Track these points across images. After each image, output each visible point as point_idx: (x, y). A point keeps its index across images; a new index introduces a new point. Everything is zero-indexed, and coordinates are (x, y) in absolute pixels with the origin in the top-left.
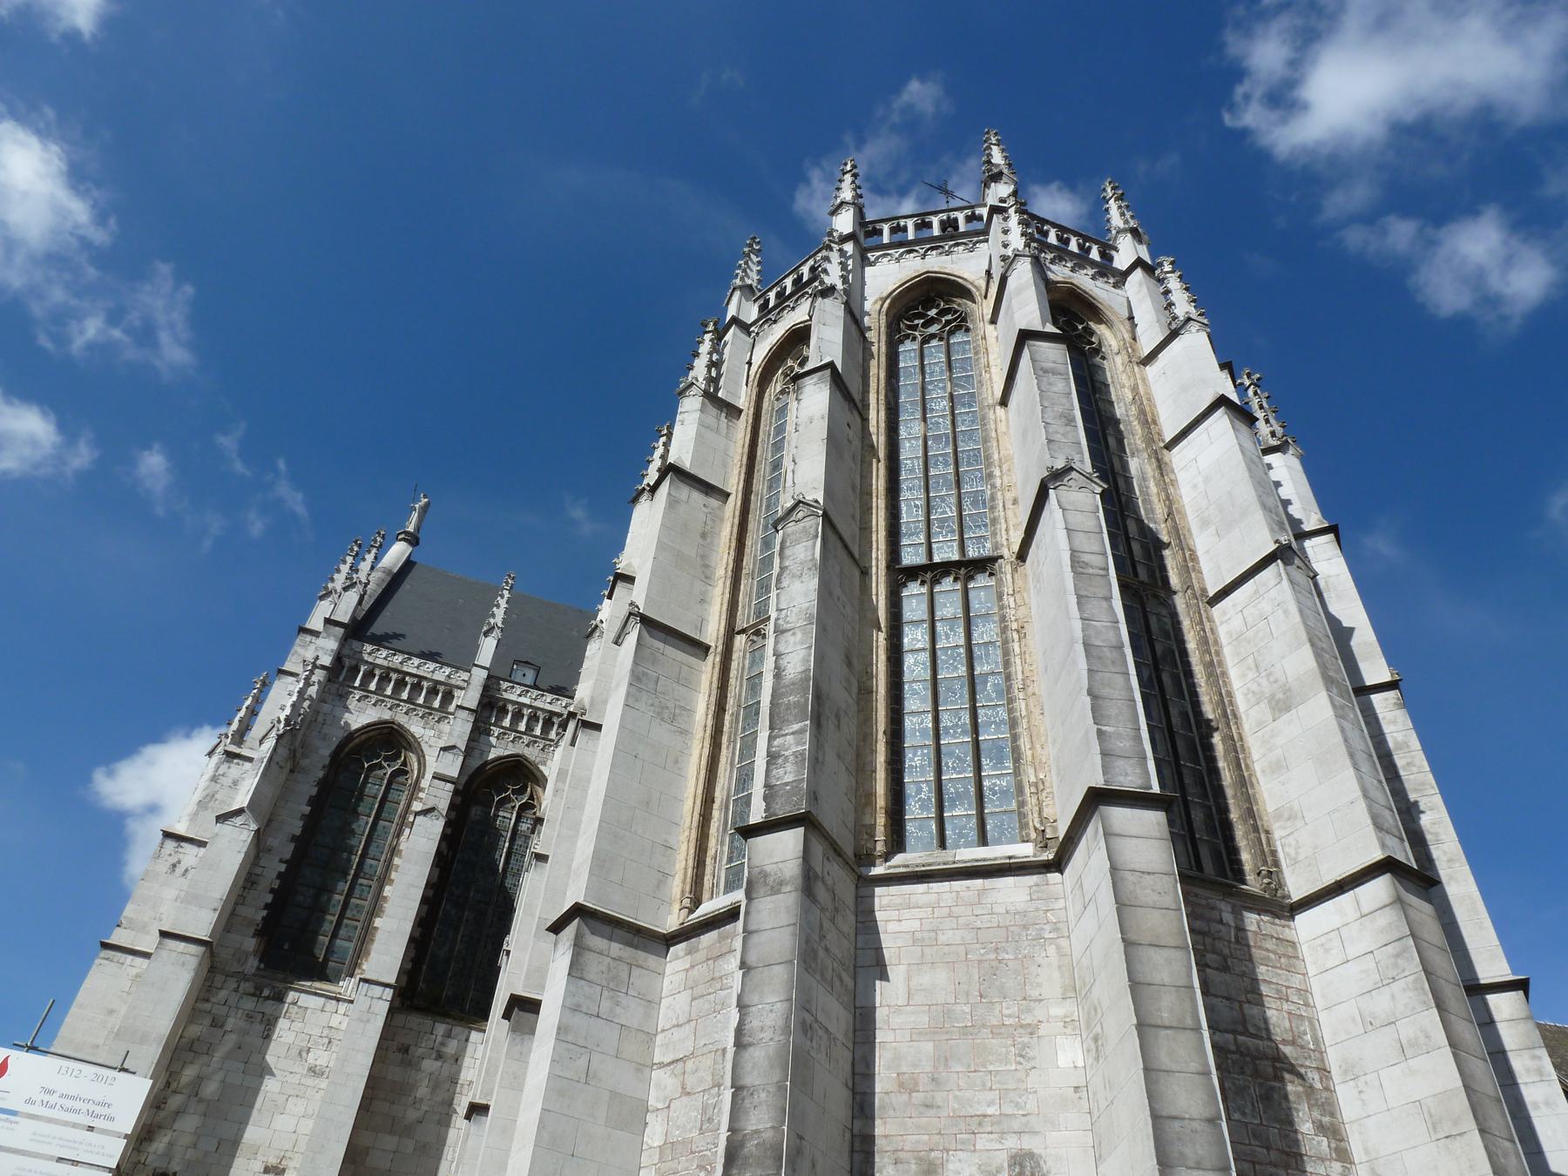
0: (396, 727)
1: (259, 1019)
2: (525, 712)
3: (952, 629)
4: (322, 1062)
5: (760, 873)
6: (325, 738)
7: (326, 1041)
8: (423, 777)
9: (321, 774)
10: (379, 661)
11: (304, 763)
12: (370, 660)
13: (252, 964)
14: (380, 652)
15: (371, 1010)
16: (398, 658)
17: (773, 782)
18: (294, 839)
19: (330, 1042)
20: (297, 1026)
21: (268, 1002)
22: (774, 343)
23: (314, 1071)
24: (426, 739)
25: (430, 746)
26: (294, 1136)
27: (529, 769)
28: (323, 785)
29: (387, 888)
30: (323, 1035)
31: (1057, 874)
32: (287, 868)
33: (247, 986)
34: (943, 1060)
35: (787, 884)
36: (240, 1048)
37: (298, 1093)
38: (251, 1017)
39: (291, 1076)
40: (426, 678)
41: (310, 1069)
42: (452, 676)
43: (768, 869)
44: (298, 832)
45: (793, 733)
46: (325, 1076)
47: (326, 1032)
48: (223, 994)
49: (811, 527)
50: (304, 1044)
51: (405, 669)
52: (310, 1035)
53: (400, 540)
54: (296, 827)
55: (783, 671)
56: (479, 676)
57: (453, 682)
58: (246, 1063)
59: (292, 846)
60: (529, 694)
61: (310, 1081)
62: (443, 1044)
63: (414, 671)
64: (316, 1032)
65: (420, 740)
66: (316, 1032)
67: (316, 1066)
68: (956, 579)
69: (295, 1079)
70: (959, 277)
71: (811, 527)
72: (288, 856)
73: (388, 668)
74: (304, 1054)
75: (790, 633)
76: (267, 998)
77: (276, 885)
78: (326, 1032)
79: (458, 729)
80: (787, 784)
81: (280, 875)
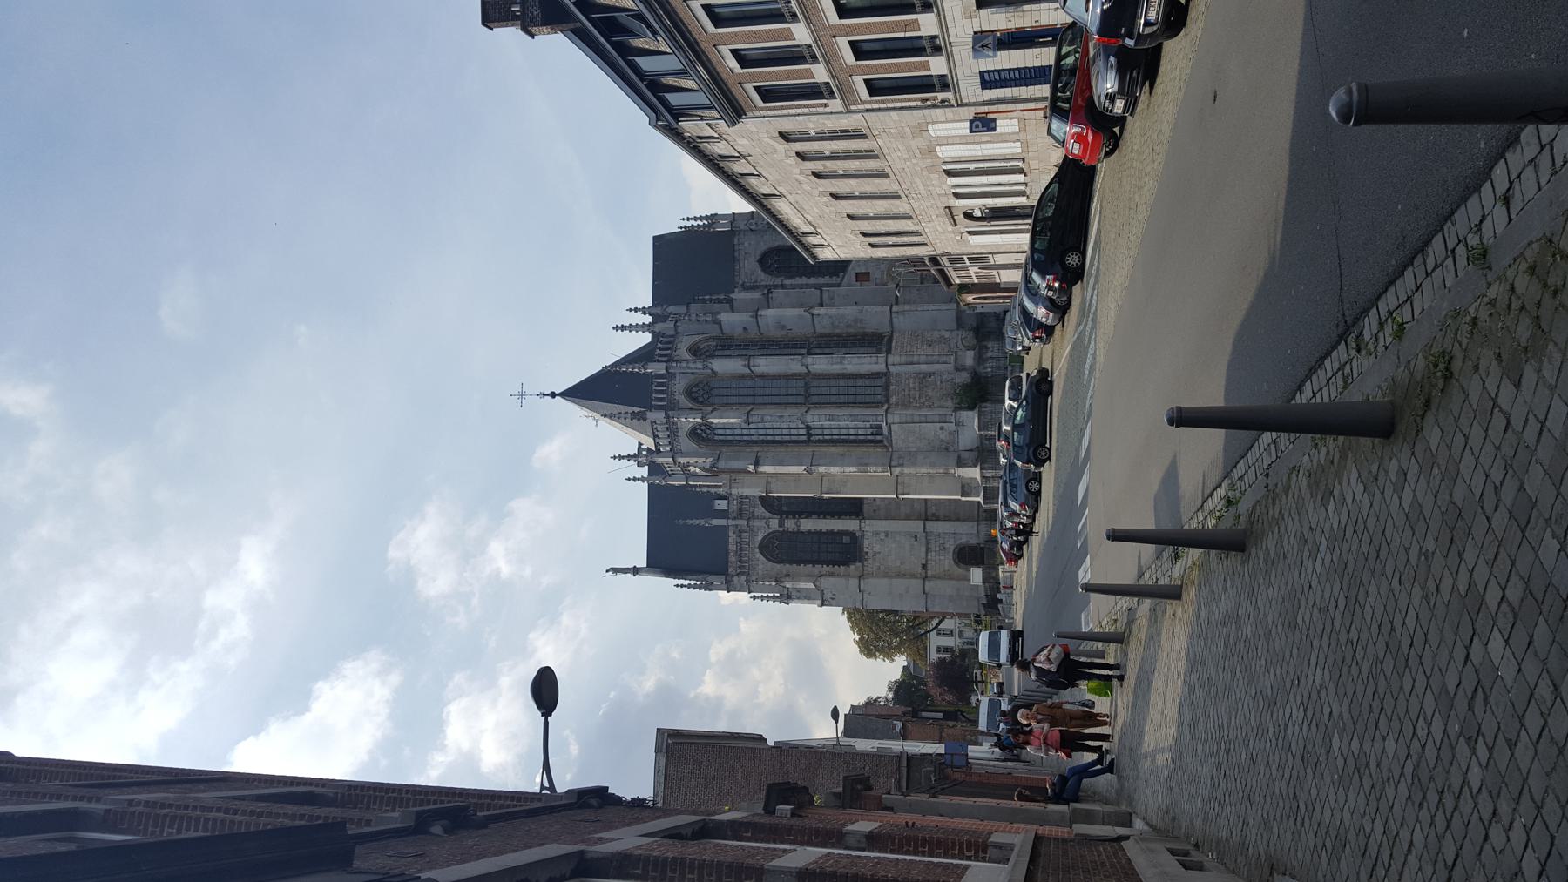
9: (788, 565)
11: (785, 572)
13: (859, 564)
18: (814, 566)
23: (887, 536)
28: (791, 563)
33: (866, 563)
34: (925, 438)
44: (811, 565)
48: (870, 569)
54: (809, 566)
56: (731, 522)
61: (890, 536)
66: (875, 539)
79: (756, 523)
81: (828, 566)
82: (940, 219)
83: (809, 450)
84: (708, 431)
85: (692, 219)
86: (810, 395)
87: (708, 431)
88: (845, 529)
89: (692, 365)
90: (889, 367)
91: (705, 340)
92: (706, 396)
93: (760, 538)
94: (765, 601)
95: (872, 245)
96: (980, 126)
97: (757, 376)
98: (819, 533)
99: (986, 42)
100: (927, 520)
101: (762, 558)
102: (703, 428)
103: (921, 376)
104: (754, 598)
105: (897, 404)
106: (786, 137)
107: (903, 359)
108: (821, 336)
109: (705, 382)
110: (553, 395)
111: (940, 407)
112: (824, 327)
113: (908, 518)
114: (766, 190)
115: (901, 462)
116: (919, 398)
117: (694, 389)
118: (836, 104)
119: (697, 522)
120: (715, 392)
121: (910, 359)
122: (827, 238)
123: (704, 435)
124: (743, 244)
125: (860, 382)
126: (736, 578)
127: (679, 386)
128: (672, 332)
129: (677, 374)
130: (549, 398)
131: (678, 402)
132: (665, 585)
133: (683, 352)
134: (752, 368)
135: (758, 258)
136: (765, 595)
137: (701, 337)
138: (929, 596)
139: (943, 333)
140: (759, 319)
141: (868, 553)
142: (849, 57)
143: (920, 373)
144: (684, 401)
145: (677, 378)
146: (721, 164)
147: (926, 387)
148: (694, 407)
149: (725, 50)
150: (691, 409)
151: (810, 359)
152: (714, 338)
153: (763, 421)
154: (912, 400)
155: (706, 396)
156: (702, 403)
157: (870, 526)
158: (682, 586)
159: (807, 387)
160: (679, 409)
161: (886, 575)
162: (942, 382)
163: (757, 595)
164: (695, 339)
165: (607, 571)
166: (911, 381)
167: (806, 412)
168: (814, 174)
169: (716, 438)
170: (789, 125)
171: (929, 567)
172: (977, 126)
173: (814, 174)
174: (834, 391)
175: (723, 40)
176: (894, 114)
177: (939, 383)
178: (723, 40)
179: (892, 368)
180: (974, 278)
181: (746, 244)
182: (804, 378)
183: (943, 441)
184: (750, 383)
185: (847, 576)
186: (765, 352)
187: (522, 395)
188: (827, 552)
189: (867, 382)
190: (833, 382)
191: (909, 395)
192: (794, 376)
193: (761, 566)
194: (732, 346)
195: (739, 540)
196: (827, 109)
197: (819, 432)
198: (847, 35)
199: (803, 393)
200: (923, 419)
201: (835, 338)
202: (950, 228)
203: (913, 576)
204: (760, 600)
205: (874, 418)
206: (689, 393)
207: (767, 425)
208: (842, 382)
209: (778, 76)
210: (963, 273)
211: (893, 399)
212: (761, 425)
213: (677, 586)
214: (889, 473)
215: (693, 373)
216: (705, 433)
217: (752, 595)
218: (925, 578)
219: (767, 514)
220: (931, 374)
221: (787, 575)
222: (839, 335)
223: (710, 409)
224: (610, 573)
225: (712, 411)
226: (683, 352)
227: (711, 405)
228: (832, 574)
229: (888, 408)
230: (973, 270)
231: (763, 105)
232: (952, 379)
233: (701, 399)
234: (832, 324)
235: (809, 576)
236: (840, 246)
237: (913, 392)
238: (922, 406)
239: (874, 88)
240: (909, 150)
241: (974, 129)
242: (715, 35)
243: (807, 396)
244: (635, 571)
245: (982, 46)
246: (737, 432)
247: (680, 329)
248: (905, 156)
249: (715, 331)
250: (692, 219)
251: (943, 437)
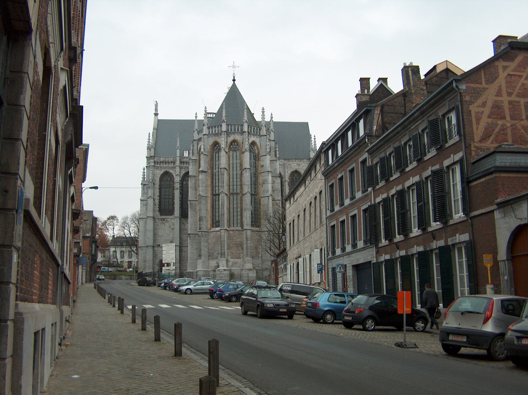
4: (173, 228)
6: (157, 177)
9: (159, 184)
11: (155, 183)
18: (158, 196)
20: (168, 223)
23: (172, 229)
28: (160, 185)
59: (158, 197)
61: (173, 230)
63: (167, 160)
64: (171, 223)
72: (159, 199)
77: (158, 204)
79: (178, 169)
81: (158, 202)
82: (297, 253)
83: (209, 195)
84: (217, 150)
85: (315, 140)
86: (233, 195)
87: (217, 150)
88: (175, 210)
89: (247, 143)
90: (245, 231)
91: (258, 148)
92: (233, 149)
93: (171, 171)
94: (142, 174)
95: (290, 224)
96: (320, 268)
97: (241, 171)
98: (173, 199)
99: (342, 269)
100: (180, 247)
101: (162, 172)
102: (219, 147)
103: (242, 244)
104: (144, 169)
105: (229, 234)
106: (321, 192)
107: (248, 236)
108: (260, 200)
109: (239, 149)
110: (234, 80)
111: (228, 252)
112: (263, 201)
113: (180, 238)
114: (307, 182)
115: (204, 236)
116: (232, 244)
117: (236, 143)
118: (329, 213)
119: (178, 143)
120: (235, 153)
121: (249, 239)
122: (293, 206)
123: (216, 148)
124: (304, 163)
125: (239, 217)
126: (152, 161)
127: (238, 137)
128: (261, 134)
129: (242, 136)
130: (233, 78)
131: (230, 137)
132: (149, 127)
133: (252, 139)
134: (245, 170)
135: (298, 170)
136: (145, 174)
137: (259, 146)
138: (146, 248)
139: (261, 254)
140: (267, 173)
142: (341, 219)
143: (243, 244)
144: (231, 138)
145: (241, 136)
146: (314, 166)
147: (237, 247)
148: (228, 143)
149: (343, 173)
150: (227, 142)
151: (249, 195)
152: (259, 152)
153: (221, 174)
154: (231, 240)
155: (233, 149)
156: (230, 147)
157: (177, 222)
158: (149, 136)
159: (237, 194)
160: (227, 137)
161: (154, 229)
162: (239, 253)
163: (145, 170)
164: (258, 144)
165: (156, 102)
166: (240, 240)
167: (226, 194)
168: (311, 202)
169: (214, 153)
170: (323, 193)
171: (159, 248)
172: (320, 266)
173: (311, 202)
174: (235, 206)
175: (346, 173)
176: (325, 235)
177: (238, 252)
178: (346, 173)
179: (244, 232)
180: (280, 266)
181: (304, 165)
182: (241, 193)
183: (213, 254)
184: (238, 168)
185: (154, 211)
186: (253, 175)
187: (234, 67)
188: (165, 202)
189: (239, 221)
190: (239, 205)
191: (233, 239)
192: (242, 188)
193: (158, 172)
194: (255, 160)
195: (170, 162)
196: (327, 210)
197: (217, 199)
198: (347, 219)
199: (234, 192)
200: (223, 245)
201: (259, 206)
202: (295, 256)
203: (154, 241)
204: (143, 171)
205: (223, 224)
206: (234, 141)
207: (220, 176)
208: (239, 210)
209: (336, 192)
210: (281, 262)
211: (231, 232)
212: (220, 173)
213: (149, 134)
214: (199, 231)
215: (243, 143)
216: (216, 149)
217: (145, 168)
218: (154, 247)
219: (182, 175)
220: (242, 249)
221: (154, 184)
222: (260, 207)
223: (227, 151)
224: (155, 103)
225: (226, 152)
226: (252, 139)
227: (229, 151)
228: (154, 204)
229: (228, 230)
230: (282, 266)
231: (329, 185)
232: (240, 258)
233: (231, 146)
234: (265, 205)
235: (154, 194)
236: (290, 211)
237: (235, 241)
238: (228, 245)
239: (333, 227)
240: (317, 240)
241: (319, 265)
242: (347, 170)
243: (233, 194)
244: (156, 114)
245: (340, 267)
246: (217, 163)
247: (262, 137)
248: (315, 239)
249: (262, 153)
250: (315, 140)
251: (215, 254)
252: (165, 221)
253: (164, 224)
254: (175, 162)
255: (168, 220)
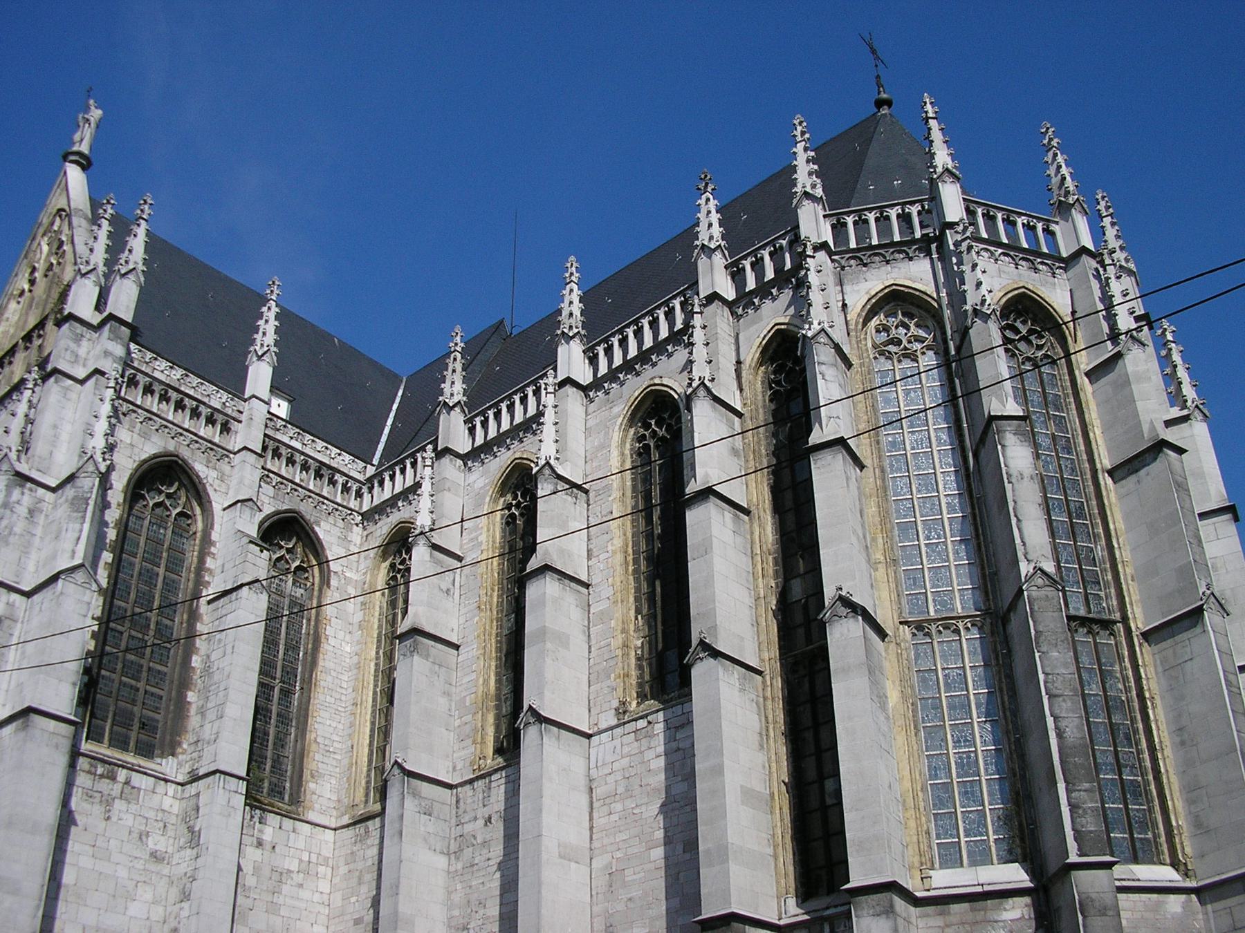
0: (180, 462)
1: (98, 800)
2: (298, 460)
3: (1090, 677)
4: (161, 847)
5: (1087, 898)
7: (161, 824)
8: (212, 527)
10: (157, 374)
12: (148, 371)
14: (158, 363)
15: (231, 804)
16: (178, 373)
17: (1079, 828)
19: (165, 826)
20: (133, 807)
21: (103, 780)
22: (873, 293)
23: (155, 856)
24: (210, 480)
25: (215, 490)
26: (148, 923)
27: (303, 527)
29: (194, 658)
30: (158, 818)
31: (693, 672)
32: (99, 628)
35: (1110, 909)
36: (86, 830)
37: (146, 879)
38: (91, 797)
39: (136, 861)
40: (204, 404)
41: (151, 854)
42: (227, 404)
43: (1094, 896)
45: (1085, 791)
46: (165, 862)
47: (160, 816)
49: (1053, 598)
50: (143, 828)
51: (182, 389)
52: (147, 819)
53: (72, 162)
55: (1064, 732)
57: (229, 411)
58: (94, 846)
60: (300, 437)
61: (153, 867)
62: (261, 831)
63: (191, 392)
64: (151, 814)
65: (205, 481)
67: (156, 851)
68: (1089, 632)
69: (139, 865)
70: (1049, 305)
71: (1053, 598)
72: (98, 613)
73: (168, 385)
74: (144, 838)
75: (1061, 699)
76: (102, 776)
78: (160, 816)
80: (1091, 832)
93: (200, 468)
141: (112, 777)
252: (117, 788)
253: (108, 802)
254: (234, 426)
255: (137, 779)
